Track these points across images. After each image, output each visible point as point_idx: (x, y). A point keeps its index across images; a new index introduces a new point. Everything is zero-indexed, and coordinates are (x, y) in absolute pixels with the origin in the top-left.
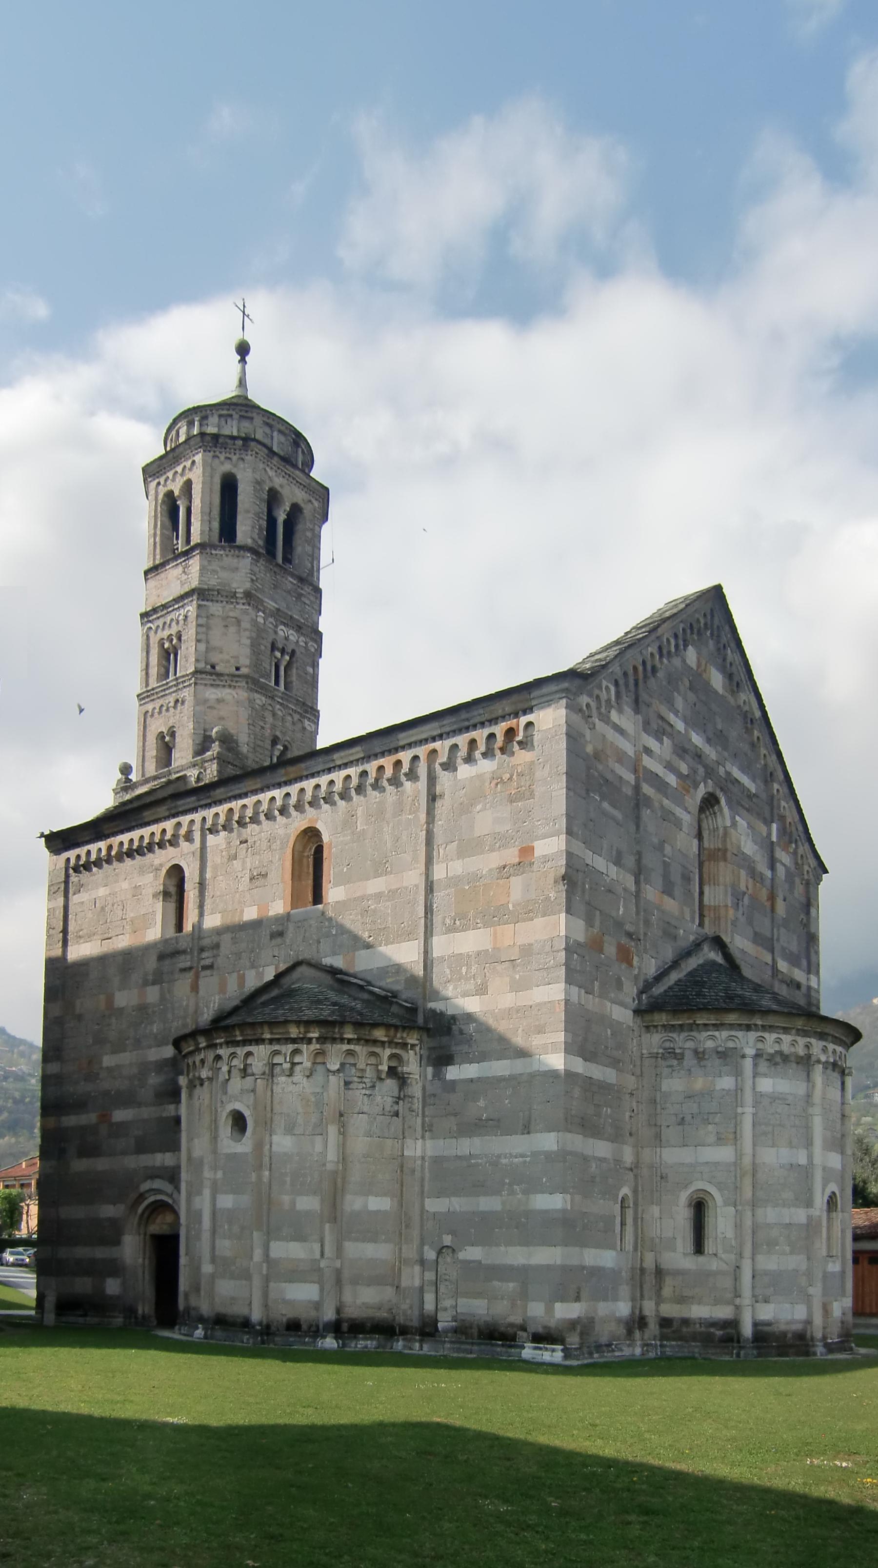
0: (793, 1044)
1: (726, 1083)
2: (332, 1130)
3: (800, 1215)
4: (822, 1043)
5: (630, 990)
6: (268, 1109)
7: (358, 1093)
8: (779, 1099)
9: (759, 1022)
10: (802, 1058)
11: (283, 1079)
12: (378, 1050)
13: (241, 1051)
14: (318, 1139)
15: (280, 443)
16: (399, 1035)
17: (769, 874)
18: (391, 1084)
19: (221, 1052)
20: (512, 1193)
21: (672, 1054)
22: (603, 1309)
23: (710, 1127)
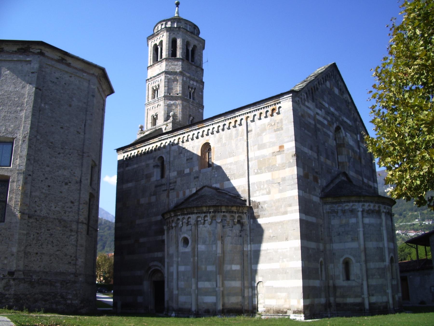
0: (374, 206)
1: (353, 220)
2: (219, 243)
4: (384, 206)
5: (318, 191)
6: (196, 236)
7: (227, 230)
9: (363, 200)
11: (201, 226)
12: (234, 215)
13: (186, 217)
14: (214, 246)
15: (190, 28)
16: (241, 209)
17: (358, 151)
18: (238, 226)
19: (179, 217)
20: (283, 261)
21: (334, 212)
23: (349, 236)
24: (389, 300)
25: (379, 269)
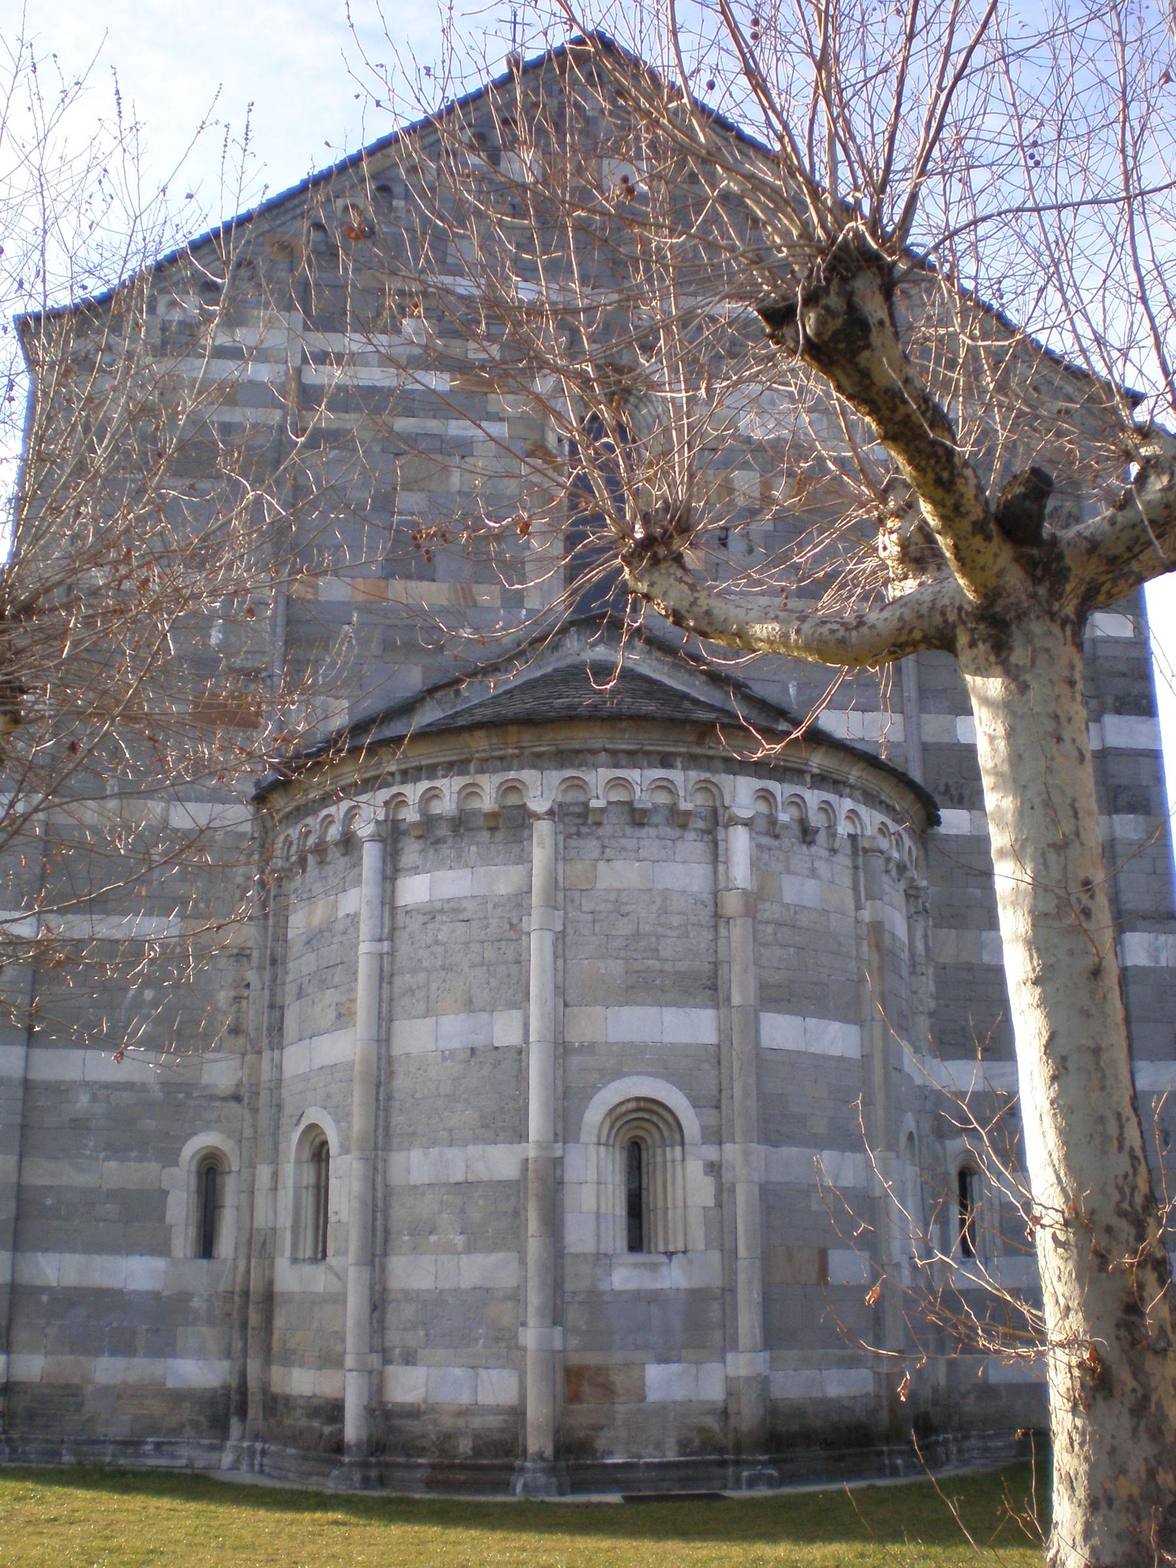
0: (470, 791)
3: (501, 1162)
8: (442, 911)
10: (494, 815)
22: (107, 1370)
24: (523, 1397)
25: (465, 1187)
